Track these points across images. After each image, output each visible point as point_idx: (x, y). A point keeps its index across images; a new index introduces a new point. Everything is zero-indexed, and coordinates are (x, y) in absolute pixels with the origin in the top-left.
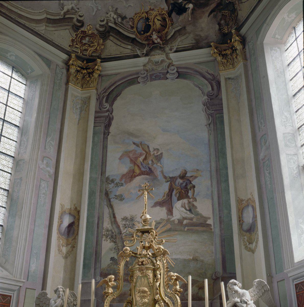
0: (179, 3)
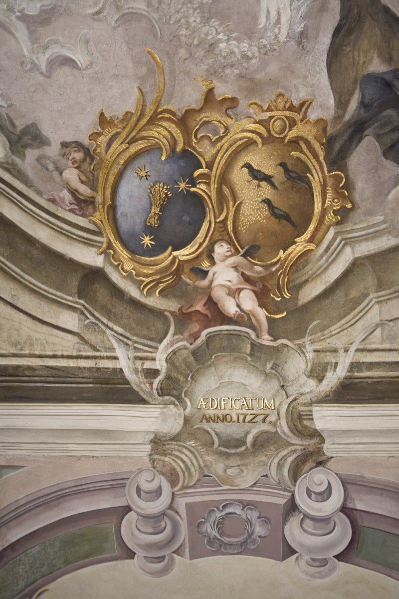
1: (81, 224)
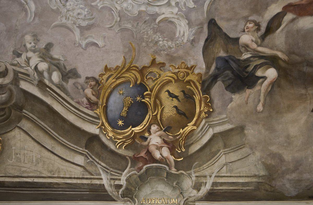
0: (241, 60)
1: (90, 114)
